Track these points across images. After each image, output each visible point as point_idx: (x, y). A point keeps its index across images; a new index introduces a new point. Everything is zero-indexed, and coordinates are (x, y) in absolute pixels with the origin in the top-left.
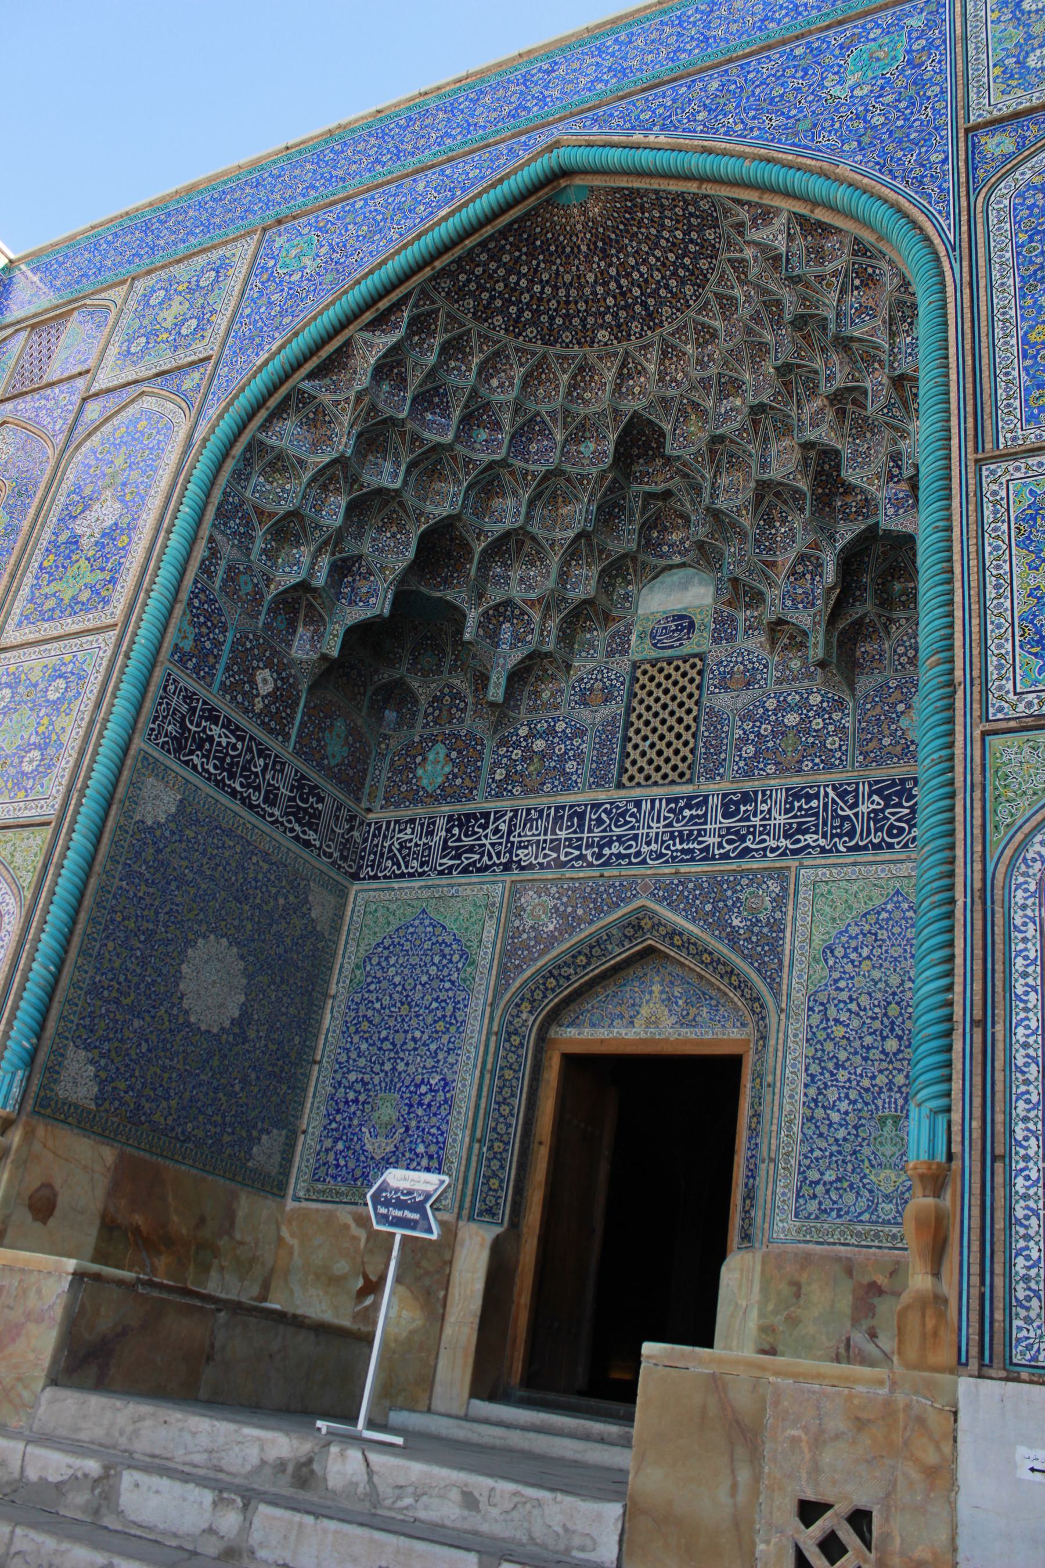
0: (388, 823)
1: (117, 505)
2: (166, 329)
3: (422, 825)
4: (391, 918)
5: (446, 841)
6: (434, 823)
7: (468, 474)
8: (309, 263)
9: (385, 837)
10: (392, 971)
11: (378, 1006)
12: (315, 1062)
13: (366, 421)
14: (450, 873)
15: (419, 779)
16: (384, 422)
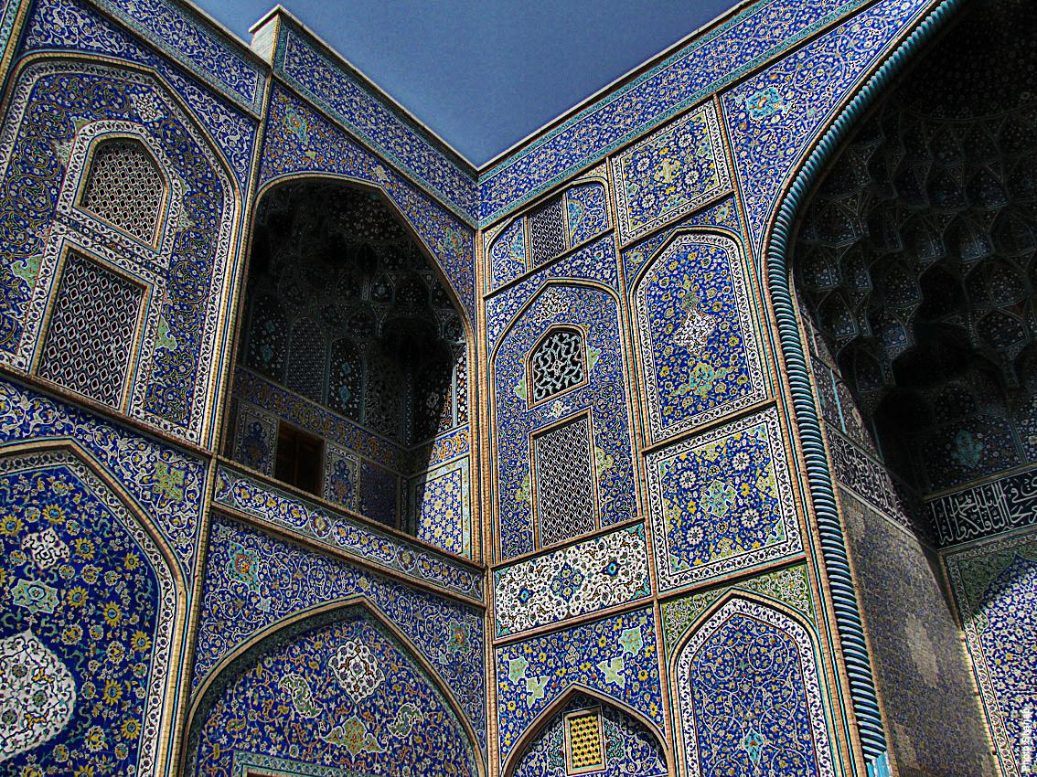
0: (946, 500)
1: (708, 317)
2: (669, 185)
3: (980, 494)
4: (988, 569)
5: (1009, 500)
6: (990, 490)
7: (942, 227)
8: (782, 107)
9: (949, 511)
10: (1012, 609)
11: (1013, 638)
12: (976, 694)
13: (870, 208)
14: (1027, 523)
15: (957, 460)
16: (881, 206)
